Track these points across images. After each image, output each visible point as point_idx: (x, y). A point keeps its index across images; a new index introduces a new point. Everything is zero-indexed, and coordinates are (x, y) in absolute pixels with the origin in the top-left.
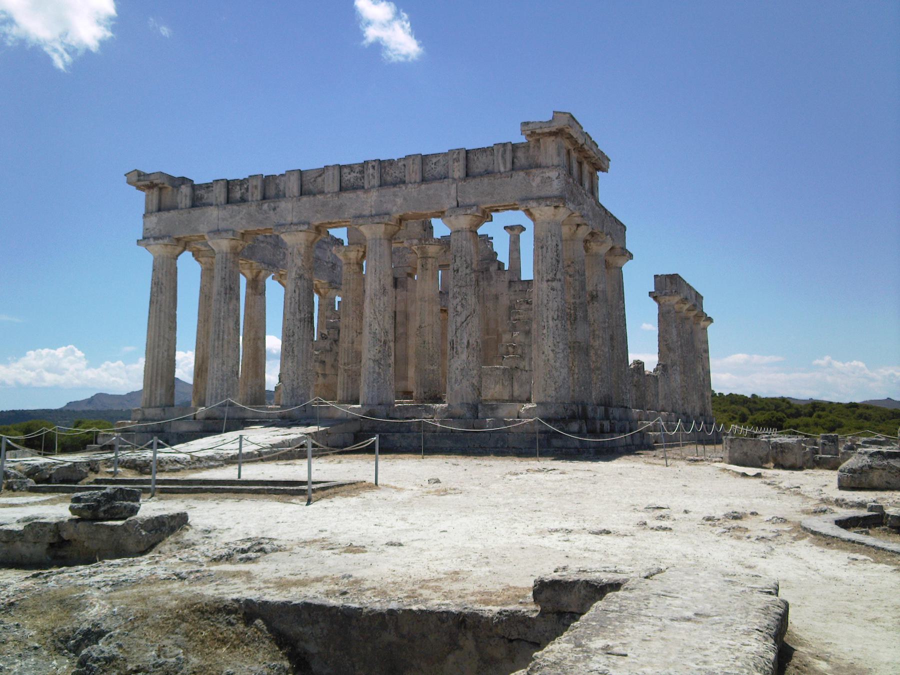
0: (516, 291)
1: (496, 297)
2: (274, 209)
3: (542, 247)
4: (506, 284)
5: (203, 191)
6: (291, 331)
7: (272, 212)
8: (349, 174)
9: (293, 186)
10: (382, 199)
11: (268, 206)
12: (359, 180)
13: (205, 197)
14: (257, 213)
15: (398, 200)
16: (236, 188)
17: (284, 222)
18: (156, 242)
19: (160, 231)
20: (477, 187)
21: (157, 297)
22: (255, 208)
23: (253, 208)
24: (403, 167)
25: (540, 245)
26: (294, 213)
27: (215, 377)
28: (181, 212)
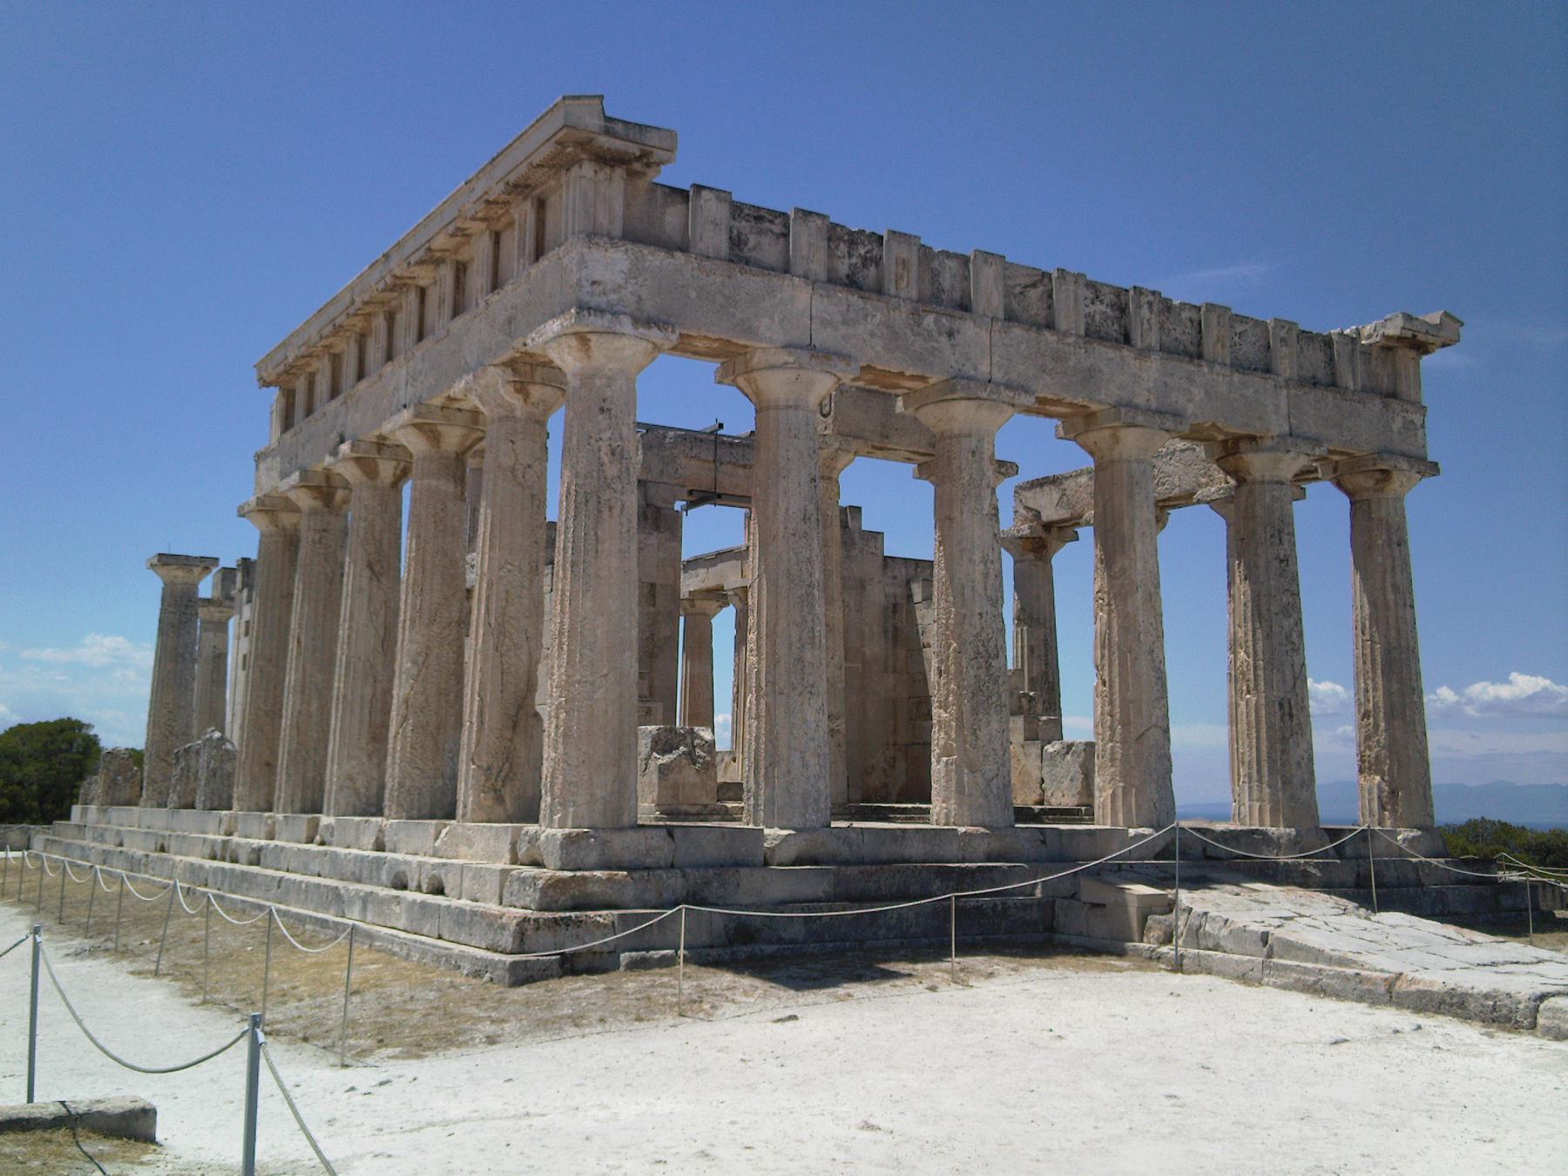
0: (895, 578)
1: (862, 585)
2: (950, 334)
3: (1399, 545)
4: (879, 561)
5: (744, 223)
6: (992, 643)
7: (944, 339)
8: (1093, 303)
9: (989, 293)
10: (1168, 382)
11: (936, 321)
12: (1109, 322)
13: (751, 244)
14: (909, 333)
15: (1195, 391)
16: (837, 247)
17: (972, 373)
18: (641, 330)
19: (639, 296)
20: (1318, 406)
21: (622, 493)
22: (904, 316)
23: (901, 317)
24: (1189, 324)
25: (1395, 539)
26: (994, 361)
27: (812, 744)
28: (707, 264)
